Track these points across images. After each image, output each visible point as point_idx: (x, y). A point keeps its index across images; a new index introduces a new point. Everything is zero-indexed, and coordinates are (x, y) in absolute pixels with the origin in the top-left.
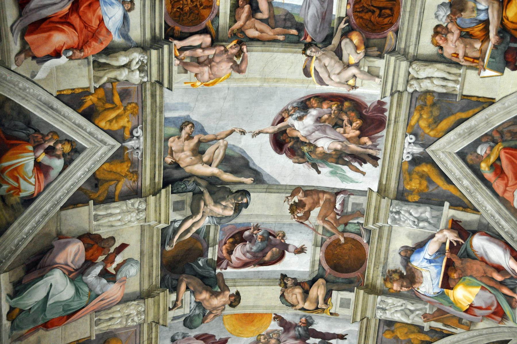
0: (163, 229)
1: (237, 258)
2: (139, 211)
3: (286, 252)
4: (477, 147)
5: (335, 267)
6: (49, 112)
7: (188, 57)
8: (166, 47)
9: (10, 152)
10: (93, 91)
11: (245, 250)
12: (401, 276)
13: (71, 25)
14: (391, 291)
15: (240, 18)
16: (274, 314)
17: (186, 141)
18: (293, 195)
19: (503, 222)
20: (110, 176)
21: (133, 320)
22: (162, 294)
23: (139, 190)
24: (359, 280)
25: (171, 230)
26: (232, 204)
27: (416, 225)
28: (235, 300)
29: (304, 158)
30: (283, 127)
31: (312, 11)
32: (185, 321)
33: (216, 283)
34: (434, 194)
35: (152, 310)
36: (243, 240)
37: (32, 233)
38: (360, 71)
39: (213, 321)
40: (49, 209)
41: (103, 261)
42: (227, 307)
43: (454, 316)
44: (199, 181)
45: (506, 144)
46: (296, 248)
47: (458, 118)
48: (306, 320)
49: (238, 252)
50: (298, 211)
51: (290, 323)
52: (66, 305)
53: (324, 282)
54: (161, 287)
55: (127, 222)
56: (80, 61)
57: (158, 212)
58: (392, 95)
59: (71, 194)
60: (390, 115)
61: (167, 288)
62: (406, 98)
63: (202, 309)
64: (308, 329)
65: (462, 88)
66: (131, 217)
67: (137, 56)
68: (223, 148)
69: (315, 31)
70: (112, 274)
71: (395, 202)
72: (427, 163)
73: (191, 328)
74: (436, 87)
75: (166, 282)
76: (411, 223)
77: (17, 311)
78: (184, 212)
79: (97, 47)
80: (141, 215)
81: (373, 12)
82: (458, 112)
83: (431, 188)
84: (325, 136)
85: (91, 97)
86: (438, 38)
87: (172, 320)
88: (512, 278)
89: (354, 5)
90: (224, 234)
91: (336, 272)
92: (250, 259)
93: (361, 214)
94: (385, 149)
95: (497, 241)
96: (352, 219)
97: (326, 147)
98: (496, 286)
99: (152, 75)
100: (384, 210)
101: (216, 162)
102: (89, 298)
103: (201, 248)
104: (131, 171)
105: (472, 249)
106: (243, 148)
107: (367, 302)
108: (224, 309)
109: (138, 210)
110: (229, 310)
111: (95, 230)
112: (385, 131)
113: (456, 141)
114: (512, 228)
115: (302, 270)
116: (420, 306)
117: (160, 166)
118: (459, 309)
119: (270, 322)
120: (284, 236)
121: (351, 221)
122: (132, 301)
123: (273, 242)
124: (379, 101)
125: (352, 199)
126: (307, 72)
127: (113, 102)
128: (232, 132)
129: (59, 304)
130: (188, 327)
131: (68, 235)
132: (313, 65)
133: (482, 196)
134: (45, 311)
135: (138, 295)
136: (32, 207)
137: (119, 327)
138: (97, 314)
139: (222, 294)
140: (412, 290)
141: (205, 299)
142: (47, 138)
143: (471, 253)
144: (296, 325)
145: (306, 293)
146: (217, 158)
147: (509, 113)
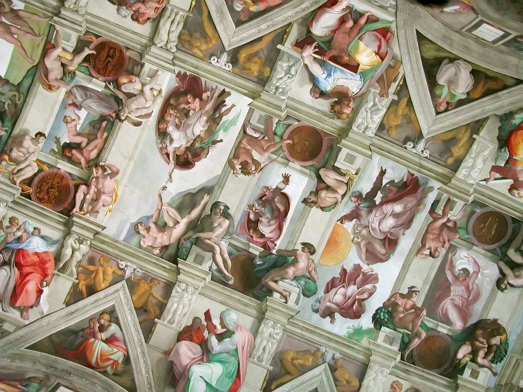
1: (270, 232)
2: (185, 290)
4: (235, 10)
6: (74, 316)
8: (74, 219)
9: (88, 353)
14: (350, 116)
15: (79, 159)
17: (150, 233)
18: (233, 168)
19: (303, 6)
20: (144, 299)
22: (268, 303)
23: (168, 283)
24: (331, 140)
25: (216, 273)
26: (220, 218)
28: (308, 249)
29: (204, 149)
33: (285, 257)
34: (268, 54)
36: (257, 222)
39: (319, 272)
48: (355, 197)
49: (266, 229)
51: (352, 211)
52: (226, 375)
53: (323, 169)
58: (174, 65)
61: (266, 297)
62: (180, 55)
63: (302, 278)
65: (183, 10)
67: (71, 241)
68: (170, 208)
69: (109, 108)
71: (266, 88)
74: (177, 30)
76: (289, 80)
78: (206, 259)
79: (50, 265)
81: (109, 62)
82: (201, 17)
83: (262, 55)
84: (192, 126)
85: (80, 284)
86: (141, 20)
88: (350, 13)
89: (100, 74)
98: (358, 28)
99: (87, 236)
101: (178, 218)
107: (355, 140)
108: (313, 261)
110: (316, 257)
112: (202, 78)
113: (226, 25)
116: (371, 97)
118: (378, 66)
120: (267, 188)
121: (274, 130)
124: (176, 76)
125: (254, 121)
126: (137, 124)
127: (92, 272)
128: (160, 196)
129: (221, 379)
133: (278, 17)
137: (275, 346)
141: (294, 272)
144: (357, 207)
145: (328, 188)
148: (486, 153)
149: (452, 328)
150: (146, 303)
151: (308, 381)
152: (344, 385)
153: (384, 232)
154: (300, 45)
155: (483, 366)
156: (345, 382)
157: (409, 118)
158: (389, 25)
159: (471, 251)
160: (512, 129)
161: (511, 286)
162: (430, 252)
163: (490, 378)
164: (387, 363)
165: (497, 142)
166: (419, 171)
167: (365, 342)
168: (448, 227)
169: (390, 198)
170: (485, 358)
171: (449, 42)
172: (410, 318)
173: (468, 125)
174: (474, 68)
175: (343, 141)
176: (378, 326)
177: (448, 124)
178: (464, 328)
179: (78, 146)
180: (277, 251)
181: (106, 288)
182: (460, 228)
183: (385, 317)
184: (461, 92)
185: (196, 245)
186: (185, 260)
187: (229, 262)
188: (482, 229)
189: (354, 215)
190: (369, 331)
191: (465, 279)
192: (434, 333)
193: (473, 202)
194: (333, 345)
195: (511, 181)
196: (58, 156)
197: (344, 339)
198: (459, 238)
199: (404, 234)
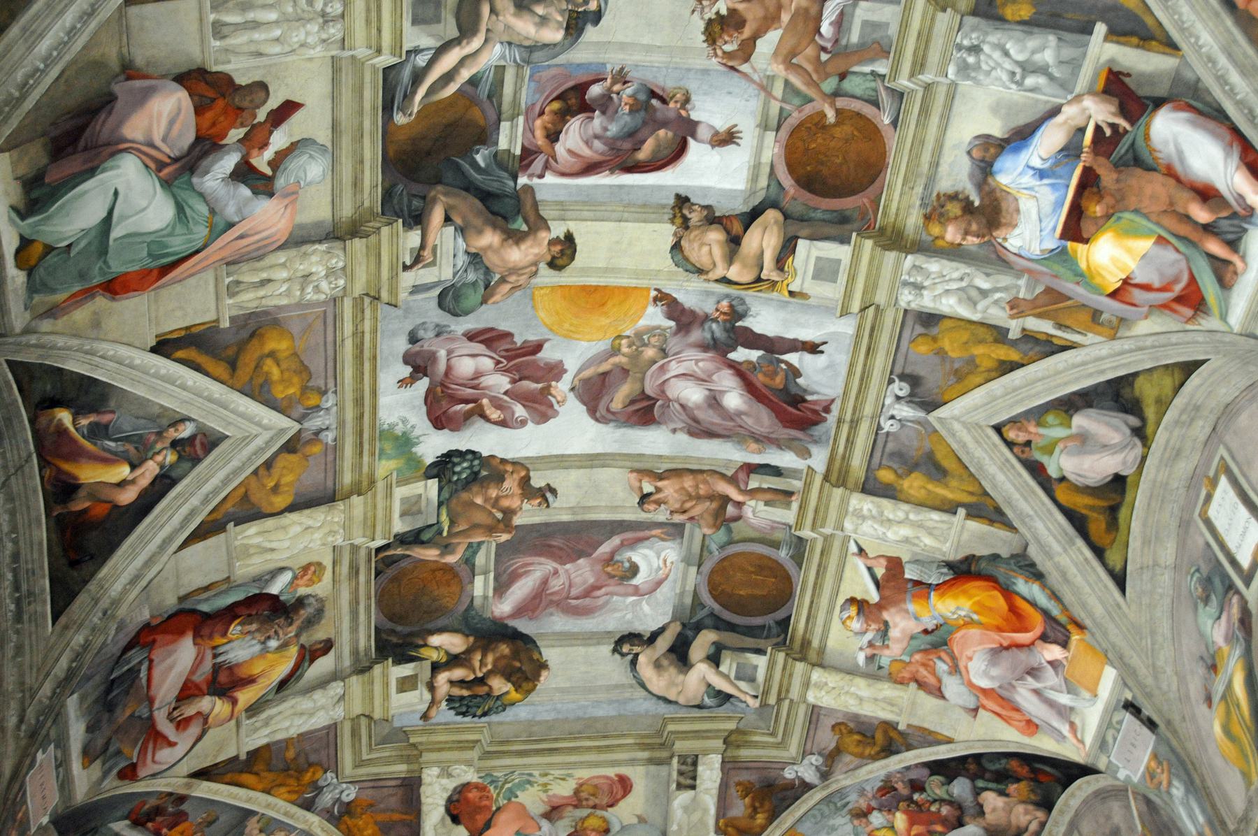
0: (387, 70)
1: (570, 152)
2: (326, 19)
3: (690, 140)
5: (810, 182)
11: (590, 132)
12: (968, 208)
14: (940, 243)
16: (656, 289)
19: (1235, 77)
21: (317, 289)
22: (385, 231)
24: (864, 214)
25: (406, 73)
26: (562, 12)
27: (1017, 83)
33: (519, 211)
35: (364, 268)
36: (586, 108)
37: (59, 57)
39: (510, 300)
41: (239, 141)
42: (543, 267)
46: (717, 133)
48: (731, 306)
50: (727, 38)
51: (693, 312)
52: (155, 242)
54: (383, 213)
55: (296, 46)
57: (374, 25)
63: (482, 271)
64: (734, 327)
66: (307, 34)
70: (263, 175)
71: (971, 21)
75: (395, 201)
76: (1005, 77)
77: (37, 250)
78: (437, 28)
80: (332, 31)
87: (411, 293)
88: (1234, 215)
90: (539, 90)
91: (809, 195)
92: (602, 154)
93: (882, 50)
95: (1212, 125)
96: (860, 63)
98: (1194, 236)
100: (941, 41)
102: (211, 231)
103: (482, 122)
105: (1148, 145)
107: (879, 268)
108: (536, 273)
109: (323, 16)
110: (547, 276)
111: (216, 64)
115: (727, 185)
116: (1005, 280)
118: (1097, 290)
119: (645, 308)
120: (687, 100)
121: (856, 69)
122: (314, 242)
123: (659, 115)
129: (139, 239)
130: (449, 312)
131: (151, 71)
134: (106, 253)
137: (284, 302)
138: (232, 268)
139: (531, 237)
141: (490, 247)
143: (1145, 155)
144: (706, 318)
145: (735, 242)
148: (928, 541)
149: (491, 600)
151: (232, 411)
152: (264, 486)
153: (663, 392)
155: (431, 687)
156: (272, 484)
159: (682, 566)
160: (1001, 579)
161: (634, 663)
162: (649, 495)
163: (413, 712)
165: (960, 556)
166: (840, 421)
167: (386, 467)
168: (723, 508)
169: (755, 380)
171: (1184, 417)
172: (480, 518)
173: (986, 494)
174: (1129, 480)
175: (868, 244)
176: (435, 471)
177: (977, 455)
178: (501, 619)
180: (525, 186)
183: (459, 473)
184: (1061, 463)
187: (452, 89)
188: (743, 570)
189: (683, 318)
190: (414, 461)
191: (613, 577)
193: (800, 539)
194: (350, 414)
195: (873, 596)
198: (704, 536)
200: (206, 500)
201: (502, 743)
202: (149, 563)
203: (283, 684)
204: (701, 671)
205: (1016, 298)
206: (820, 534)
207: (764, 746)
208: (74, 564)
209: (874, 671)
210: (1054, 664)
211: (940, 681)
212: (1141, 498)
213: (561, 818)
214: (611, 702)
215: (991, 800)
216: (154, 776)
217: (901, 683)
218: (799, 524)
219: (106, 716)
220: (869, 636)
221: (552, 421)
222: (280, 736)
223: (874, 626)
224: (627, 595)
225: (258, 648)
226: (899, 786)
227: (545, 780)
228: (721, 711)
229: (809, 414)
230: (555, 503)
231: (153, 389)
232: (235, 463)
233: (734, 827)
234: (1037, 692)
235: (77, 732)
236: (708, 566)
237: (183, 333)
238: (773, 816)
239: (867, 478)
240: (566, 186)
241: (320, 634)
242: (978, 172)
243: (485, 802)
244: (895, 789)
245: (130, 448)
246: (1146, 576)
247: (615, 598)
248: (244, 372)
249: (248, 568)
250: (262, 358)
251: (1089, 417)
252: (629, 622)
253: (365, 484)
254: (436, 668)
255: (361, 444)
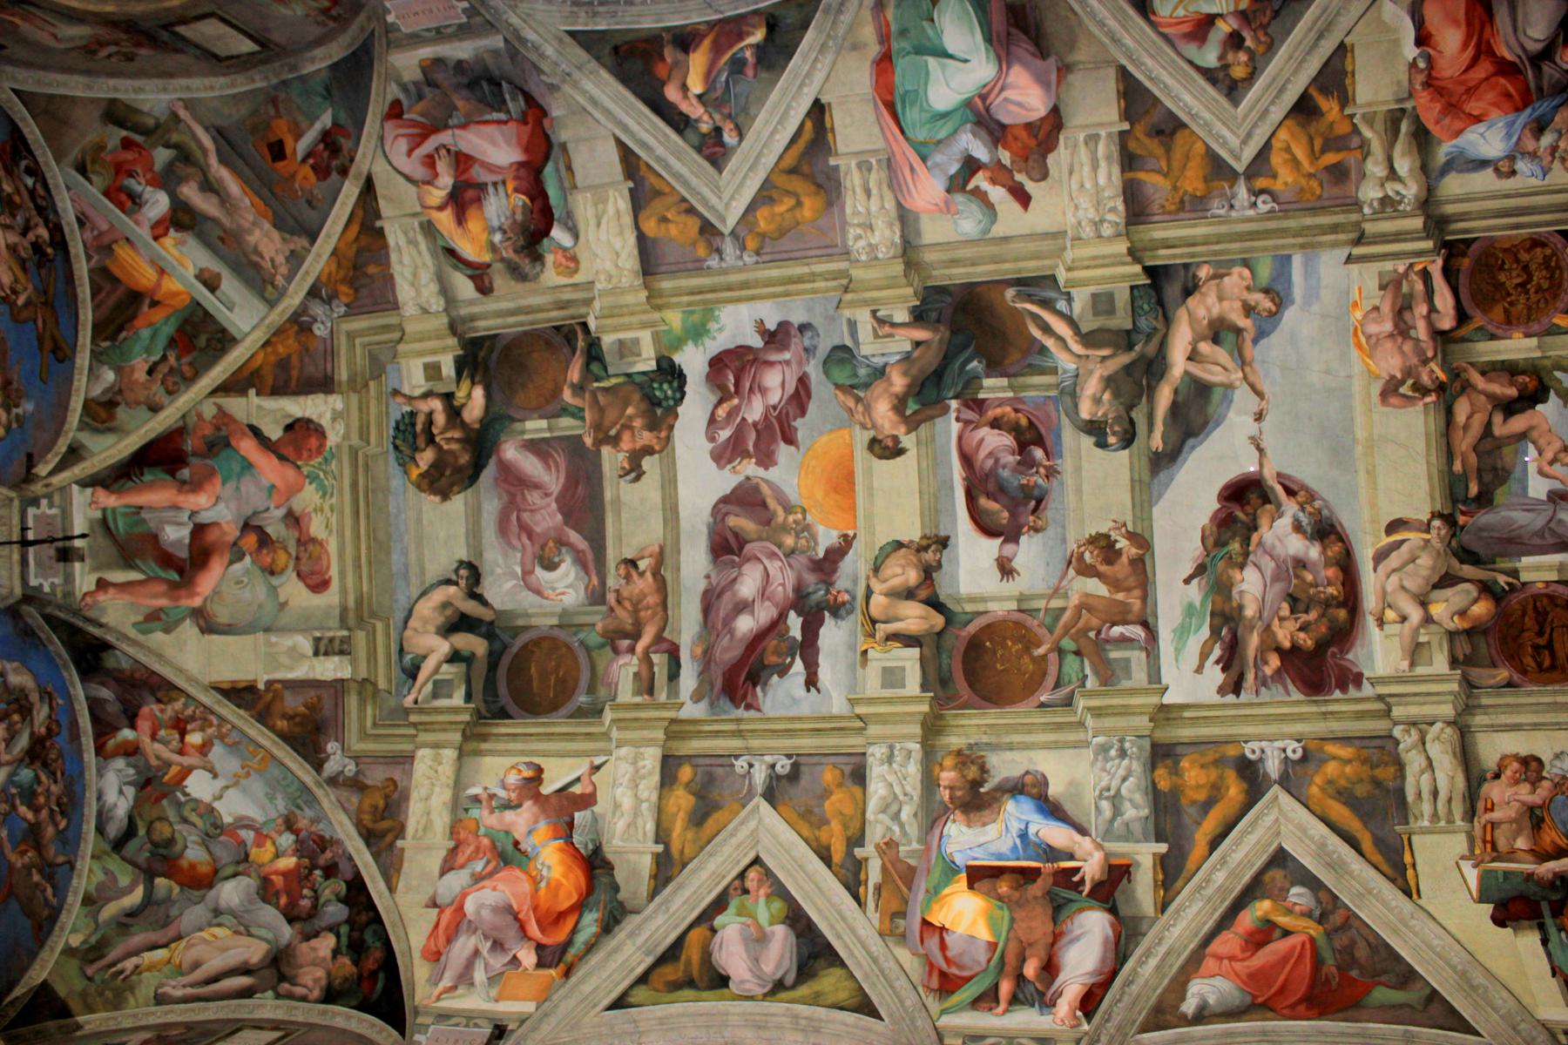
0: (1053, 278)
1: (982, 440)
2: (1097, 224)
3: (1001, 540)
4: (1303, 884)
5: (974, 647)
7: (1412, 287)
10: (1348, 111)
11: (1001, 455)
12: (976, 784)
13: (1474, 61)
14: (937, 769)
15: (1490, 380)
17: (1238, 304)
18: (1132, 536)
19: (1153, 962)
21: (859, 237)
22: (910, 291)
25: (1051, 294)
26: (1105, 415)
28: (887, 447)
30: (1276, 497)
31: (1520, 517)
32: (844, 348)
36: (1022, 447)
37: (1086, 13)
38: (1418, 629)
40: (1123, 45)
43: (907, 902)
44: (1156, 340)
45: (1322, 942)
46: (1010, 560)
47: (1359, 835)
48: (844, 603)
49: (995, 443)
51: (834, 571)
52: (916, 96)
56: (1406, 84)
58: (1380, 698)
59: (1148, 84)
60: (1337, 701)
62: (1378, 726)
65: (1424, 831)
67: (1411, 190)
69: (1481, 529)
70: (966, 182)
71: (1147, 744)
72: (1247, 792)
73: (825, 363)
74: (1415, 781)
76: (1104, 784)
81: (1540, 634)
82: (1373, 835)
85: (1336, 108)
86: (1515, 765)
87: (849, 321)
88: (1042, 994)
94: (1260, 704)
95: (1111, 955)
96: (1092, 663)
97: (1244, 587)
101: (1196, 370)
104: (1187, 198)
106: (1227, 422)
107: (902, 722)
108: (864, 427)
110: (862, 438)
112: (1301, 697)
114: (1147, 981)
116: (913, 830)
117: (1193, 255)
118: (927, 906)
119: (836, 528)
120: (1037, 530)
121: (1086, 662)
122: (902, 231)
123: (1021, 509)
125: (1137, 657)
126: (1394, 526)
127: (1323, 151)
128: (1260, 394)
132: (1412, 535)
133: (1198, 913)
135: (914, 243)
136: (1131, 12)
137: (848, 211)
140: (946, 809)
141: (891, 384)
142: (1260, 34)
145: (909, 594)
146: (1205, 370)
147: (1395, 931)
148: (621, 825)
150: (1168, 151)
152: (668, 209)
153: (749, 560)
154: (1118, 873)
155: (426, 395)
157: (811, 824)
158: (947, 1004)
159: (559, 610)
160: (592, 899)
161: (448, 582)
162: (635, 566)
163: (401, 382)
164: (608, 301)
165: (610, 857)
166: (739, 721)
167: (674, 319)
168: (626, 635)
170: (430, 414)
172: (611, 415)
173: (684, 865)
174: (725, 991)
175: (925, 708)
176: (665, 365)
178: (498, 452)
179: (1510, 408)
181: (1273, 134)
182: (602, 646)
183: (661, 389)
184: (730, 926)
185: (1128, 332)
186: (1132, 288)
187: (1036, 333)
190: (678, 344)
191: (542, 548)
192: (550, 408)
193: (601, 711)
194: (734, 278)
195: (547, 789)
196: (1547, 363)
197: (718, 301)
199: (708, 577)
200: (659, 159)
201: (367, 466)
202: (607, 112)
203: (451, 252)
204: (443, 647)
205: (897, 845)
206: (610, 728)
207: (362, 719)
208: (616, 50)
209: (460, 805)
210: (515, 961)
211: (462, 867)
212: (709, 1005)
213: (287, 526)
214: (406, 566)
215: (325, 945)
216: (382, 138)
217: (452, 833)
218: (617, 707)
219: (465, 81)
220: (502, 793)
221: (714, 465)
222: (394, 257)
223: (513, 795)
224: (523, 564)
225: (496, 223)
226: (328, 854)
227: (326, 508)
228: (396, 671)
229: (741, 692)
230: (625, 485)
231: (775, 106)
232: (694, 182)
233: (274, 698)
234: (476, 953)
235: (462, 50)
236: (562, 635)
237: (828, 125)
238: (285, 737)
239: (680, 757)
240: (949, 442)
241: (501, 281)
242: (1011, 784)
243: (305, 454)
244: (323, 851)
245: (718, 93)
246: (629, 1027)
247: (519, 555)
248: (782, 181)
249: (583, 207)
250: (796, 195)
251: (786, 938)
252: (492, 573)
253: (659, 301)
254: (448, 397)
255: (701, 293)
